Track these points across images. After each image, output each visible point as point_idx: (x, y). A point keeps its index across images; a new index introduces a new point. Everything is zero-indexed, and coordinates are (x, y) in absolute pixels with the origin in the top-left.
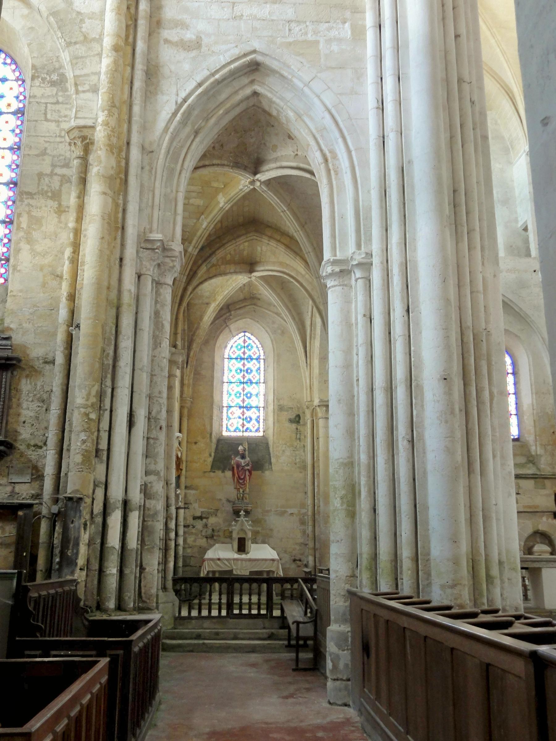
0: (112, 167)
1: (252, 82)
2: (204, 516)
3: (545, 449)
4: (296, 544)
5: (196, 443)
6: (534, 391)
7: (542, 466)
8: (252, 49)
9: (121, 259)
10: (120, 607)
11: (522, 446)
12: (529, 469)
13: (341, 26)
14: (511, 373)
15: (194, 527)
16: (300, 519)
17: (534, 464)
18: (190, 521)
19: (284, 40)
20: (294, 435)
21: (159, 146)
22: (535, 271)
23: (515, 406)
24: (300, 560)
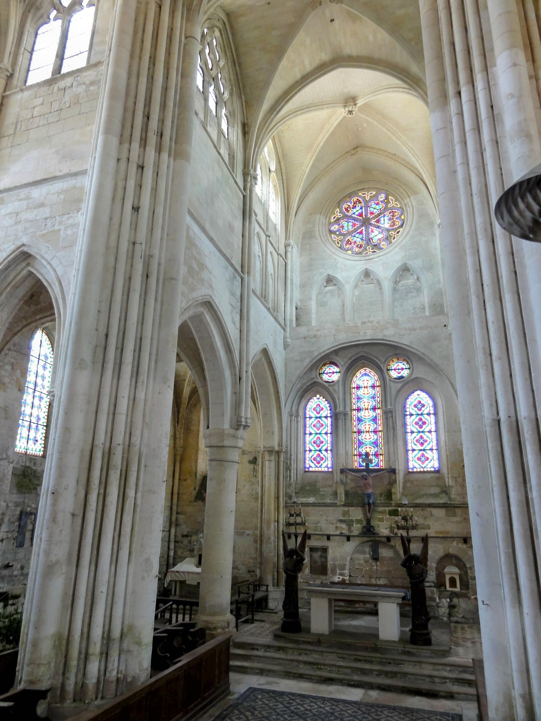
1: (28, 264)
2: (189, 534)
3: (456, 481)
4: (251, 558)
5: (185, 480)
7: (453, 496)
8: (22, 243)
11: (438, 478)
12: (441, 499)
13: (76, 215)
14: (432, 414)
15: (182, 543)
17: (447, 494)
18: (179, 538)
19: (42, 233)
20: (252, 473)
22: (445, 326)
23: (436, 442)
24: (253, 572)
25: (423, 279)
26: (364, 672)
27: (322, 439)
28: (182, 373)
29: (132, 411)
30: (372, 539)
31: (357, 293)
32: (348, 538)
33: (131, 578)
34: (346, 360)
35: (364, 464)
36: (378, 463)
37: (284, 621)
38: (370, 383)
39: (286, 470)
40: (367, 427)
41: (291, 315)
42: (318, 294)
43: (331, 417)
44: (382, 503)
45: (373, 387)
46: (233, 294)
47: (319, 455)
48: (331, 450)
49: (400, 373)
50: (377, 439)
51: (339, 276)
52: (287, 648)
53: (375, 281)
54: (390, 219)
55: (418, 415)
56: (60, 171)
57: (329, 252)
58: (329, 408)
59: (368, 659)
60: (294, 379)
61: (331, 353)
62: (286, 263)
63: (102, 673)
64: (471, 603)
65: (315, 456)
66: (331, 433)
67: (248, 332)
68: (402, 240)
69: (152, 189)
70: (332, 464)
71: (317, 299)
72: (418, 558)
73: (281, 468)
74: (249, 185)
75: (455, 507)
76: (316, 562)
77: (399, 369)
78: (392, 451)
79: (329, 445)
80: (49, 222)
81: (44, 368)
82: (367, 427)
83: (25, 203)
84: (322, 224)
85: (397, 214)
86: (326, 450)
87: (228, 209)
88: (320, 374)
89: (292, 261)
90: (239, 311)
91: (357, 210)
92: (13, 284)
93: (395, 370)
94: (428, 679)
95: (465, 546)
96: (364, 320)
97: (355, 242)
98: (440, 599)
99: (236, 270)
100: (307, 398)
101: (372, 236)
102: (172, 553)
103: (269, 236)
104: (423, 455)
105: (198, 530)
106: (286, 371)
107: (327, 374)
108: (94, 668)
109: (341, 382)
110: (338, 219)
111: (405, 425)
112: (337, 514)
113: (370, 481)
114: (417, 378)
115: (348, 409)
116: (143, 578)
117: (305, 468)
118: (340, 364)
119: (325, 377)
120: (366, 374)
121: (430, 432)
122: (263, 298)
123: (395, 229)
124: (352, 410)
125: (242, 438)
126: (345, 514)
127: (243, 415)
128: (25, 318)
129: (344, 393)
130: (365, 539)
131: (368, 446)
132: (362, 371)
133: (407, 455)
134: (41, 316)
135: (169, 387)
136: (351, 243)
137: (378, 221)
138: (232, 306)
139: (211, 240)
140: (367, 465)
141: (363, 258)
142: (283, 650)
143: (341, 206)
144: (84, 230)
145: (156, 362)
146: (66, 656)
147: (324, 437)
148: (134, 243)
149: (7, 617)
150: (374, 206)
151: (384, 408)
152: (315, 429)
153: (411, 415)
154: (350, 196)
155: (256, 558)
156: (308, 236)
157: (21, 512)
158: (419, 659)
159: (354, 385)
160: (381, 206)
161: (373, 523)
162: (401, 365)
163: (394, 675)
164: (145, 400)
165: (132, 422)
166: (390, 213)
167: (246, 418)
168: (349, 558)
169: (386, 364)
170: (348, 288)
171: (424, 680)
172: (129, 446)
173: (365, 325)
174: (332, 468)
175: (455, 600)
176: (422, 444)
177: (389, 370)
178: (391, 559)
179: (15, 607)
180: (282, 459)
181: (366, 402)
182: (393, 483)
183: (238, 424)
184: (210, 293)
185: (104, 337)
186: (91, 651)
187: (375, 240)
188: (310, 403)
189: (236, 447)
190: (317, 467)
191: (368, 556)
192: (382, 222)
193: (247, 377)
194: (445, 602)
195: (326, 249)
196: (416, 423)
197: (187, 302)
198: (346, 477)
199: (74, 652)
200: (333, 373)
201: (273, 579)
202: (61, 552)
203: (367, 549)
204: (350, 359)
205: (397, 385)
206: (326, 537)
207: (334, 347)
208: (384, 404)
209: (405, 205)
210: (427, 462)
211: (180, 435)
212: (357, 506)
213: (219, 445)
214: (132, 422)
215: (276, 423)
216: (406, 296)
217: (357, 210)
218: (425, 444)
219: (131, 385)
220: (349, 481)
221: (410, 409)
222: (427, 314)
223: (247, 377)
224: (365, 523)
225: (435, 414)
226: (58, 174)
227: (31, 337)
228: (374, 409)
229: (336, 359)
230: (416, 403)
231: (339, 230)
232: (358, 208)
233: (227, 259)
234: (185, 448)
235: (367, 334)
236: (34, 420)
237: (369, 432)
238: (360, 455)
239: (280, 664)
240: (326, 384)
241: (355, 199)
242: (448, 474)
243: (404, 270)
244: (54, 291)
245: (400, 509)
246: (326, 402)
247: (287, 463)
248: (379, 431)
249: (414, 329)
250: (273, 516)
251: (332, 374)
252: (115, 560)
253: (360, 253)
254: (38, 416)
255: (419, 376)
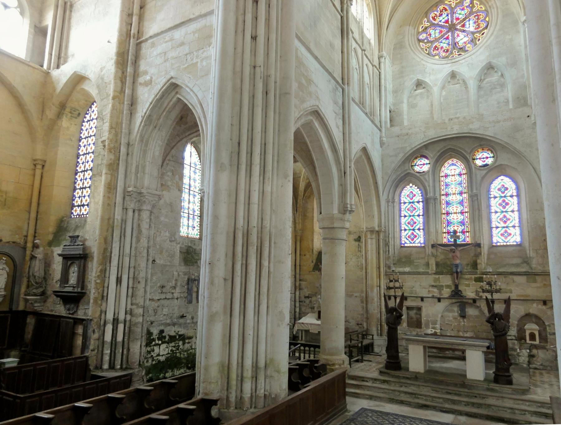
0: (111, 159)
1: (177, 93)
3: (537, 253)
6: (528, 209)
7: (534, 266)
9: (115, 203)
10: (112, 367)
16: (361, 300)
21: (136, 140)
22: (528, 116)
25: (507, 75)
26: (453, 402)
27: (415, 220)
28: (298, 172)
29: (262, 202)
30: (459, 300)
31: (444, 93)
32: (439, 300)
33: (269, 325)
34: (435, 153)
35: (452, 240)
36: (467, 238)
37: (387, 362)
38: (457, 172)
39: (386, 246)
40: (455, 209)
41: (386, 117)
42: (409, 97)
43: (422, 202)
44: (468, 272)
45: (460, 175)
46: (336, 103)
47: (413, 233)
48: (423, 229)
49: (484, 161)
50: (464, 219)
51: (427, 80)
52: (390, 381)
53: (461, 82)
54: (475, 23)
55: (502, 197)
56: (193, 14)
57: (418, 60)
58: (420, 195)
59: (457, 392)
60: (389, 172)
61: (421, 148)
62: (380, 73)
63: (254, 391)
64: (549, 354)
65: (409, 234)
66: (423, 215)
67: (350, 133)
68: (487, 41)
69: (266, 19)
70: (424, 240)
71: (408, 102)
72: (501, 315)
73: (381, 244)
74: (345, 6)
75: (536, 274)
76: (412, 318)
77: (484, 158)
78: (477, 228)
79: (421, 225)
80: (189, 57)
81: (195, 173)
82: (455, 209)
83: (170, 43)
84: (411, 34)
85: (481, 16)
86: (419, 229)
87: (329, 31)
88: (412, 166)
89: (385, 70)
90: (341, 117)
91: (443, 18)
92: (167, 109)
93: (480, 159)
94: (509, 411)
95: (544, 307)
96: (452, 117)
97: (442, 48)
98: (520, 349)
99: (337, 82)
100: (401, 187)
101: (457, 40)
102: (297, 310)
103: (365, 50)
104: (506, 231)
105: (316, 293)
106: (383, 165)
107: (418, 165)
108: (248, 387)
109: (430, 172)
110: (426, 28)
111: (489, 206)
112: (430, 280)
113: (458, 254)
114: (501, 165)
115: (437, 195)
116: (279, 325)
117: (401, 244)
118: (430, 156)
119: (417, 169)
120: (453, 164)
121: (513, 211)
122: (361, 104)
123: (479, 30)
124: (441, 195)
125: (348, 221)
126: (436, 280)
127: (349, 202)
128: (178, 135)
129: (434, 181)
130: (454, 301)
131: (456, 225)
132: (450, 161)
133: (491, 232)
134: (189, 133)
135: (289, 181)
136: (438, 49)
137: (463, 26)
138: (335, 113)
139: (316, 58)
140: (455, 241)
141: (449, 61)
142: (388, 383)
143: (428, 15)
144: (216, 60)
145: (278, 162)
146: (228, 378)
147: (416, 219)
148: (255, 67)
149: (186, 351)
150: (459, 12)
151: (470, 193)
152: (409, 212)
153: (495, 197)
154: (437, 5)
155: (362, 314)
156: (399, 46)
157: (188, 279)
158: (501, 395)
159: (442, 174)
160: (466, 11)
161: (460, 288)
162: (486, 155)
163: (479, 406)
164: (272, 193)
165: (262, 210)
166: (475, 16)
167: (351, 205)
168: (440, 316)
169: (472, 154)
170: (436, 90)
171: (506, 411)
172: (262, 228)
173: (452, 121)
174: (424, 243)
175: (535, 351)
176: (505, 222)
177: (474, 159)
178: (477, 317)
179: (190, 344)
180: (381, 237)
181: (454, 189)
182: (478, 255)
183: (344, 210)
184: (317, 104)
185: (237, 145)
186: (245, 375)
187: (461, 44)
188: (404, 191)
189: (344, 228)
190: (411, 243)
191: (456, 314)
192: (467, 26)
193: (351, 172)
194: (525, 352)
195: (415, 57)
196: (500, 204)
197: (299, 113)
198: (437, 250)
199: (234, 376)
200: (424, 164)
201: (377, 330)
202: (219, 306)
203: (456, 309)
204: (439, 151)
205: (482, 172)
206: (420, 299)
207: (424, 142)
208: (470, 189)
209: (490, 7)
210: (509, 238)
211: (299, 220)
212: (447, 274)
213: (330, 226)
214: (262, 210)
215: (375, 208)
216: (491, 92)
217: (443, 18)
218: (508, 222)
219: (260, 181)
220: (439, 254)
221: (494, 192)
222: (511, 106)
223: (351, 172)
224: (453, 288)
225: (518, 196)
226: (192, 17)
227: (183, 150)
228: (461, 193)
229: (425, 152)
230: (499, 187)
231: (427, 38)
232: (444, 16)
233: (330, 74)
234: (303, 230)
235: (454, 130)
236: (191, 212)
237: (456, 213)
238: (448, 233)
239: (385, 393)
240: (418, 174)
241: (441, 7)
242: (530, 247)
243: (489, 69)
244: (197, 112)
245: (484, 276)
246: (418, 190)
247: (386, 241)
248: (466, 212)
249: (499, 122)
250: (375, 281)
251: (422, 166)
252: (257, 312)
253: (447, 57)
254: (193, 209)
255: (503, 163)
